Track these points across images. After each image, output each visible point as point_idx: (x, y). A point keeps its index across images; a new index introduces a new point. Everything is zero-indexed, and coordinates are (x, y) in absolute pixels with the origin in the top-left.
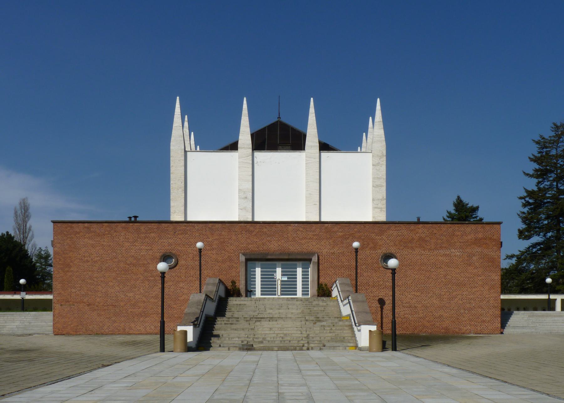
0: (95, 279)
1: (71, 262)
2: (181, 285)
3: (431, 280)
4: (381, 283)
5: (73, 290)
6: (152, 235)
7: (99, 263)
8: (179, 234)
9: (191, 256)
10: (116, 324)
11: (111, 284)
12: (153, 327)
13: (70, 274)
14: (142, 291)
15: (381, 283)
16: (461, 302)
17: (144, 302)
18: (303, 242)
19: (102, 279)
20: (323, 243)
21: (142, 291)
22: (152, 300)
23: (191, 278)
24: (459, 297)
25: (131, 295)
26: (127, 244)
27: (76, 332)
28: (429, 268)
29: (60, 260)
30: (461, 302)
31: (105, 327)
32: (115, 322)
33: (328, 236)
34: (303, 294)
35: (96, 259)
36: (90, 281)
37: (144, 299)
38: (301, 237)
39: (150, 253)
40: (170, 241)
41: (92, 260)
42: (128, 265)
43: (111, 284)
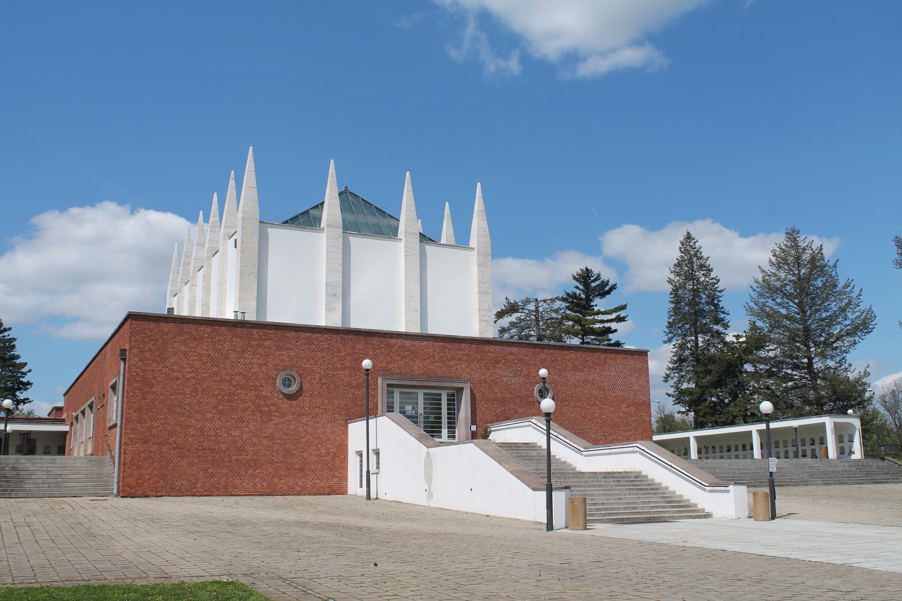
0: (187, 408)
1: (154, 378)
2: (304, 419)
5: (155, 424)
6: (268, 343)
7: (194, 382)
9: (317, 376)
12: (265, 484)
13: (150, 397)
14: (253, 429)
17: (254, 444)
18: (452, 363)
20: (473, 367)
21: (253, 429)
22: (265, 442)
23: (317, 410)
25: (237, 433)
26: (233, 355)
27: (157, 492)
29: (138, 374)
31: (199, 485)
32: (212, 475)
35: (189, 375)
36: (179, 410)
37: (255, 440)
39: (264, 369)
40: (292, 353)
41: (184, 376)
42: (234, 386)
43: (209, 415)
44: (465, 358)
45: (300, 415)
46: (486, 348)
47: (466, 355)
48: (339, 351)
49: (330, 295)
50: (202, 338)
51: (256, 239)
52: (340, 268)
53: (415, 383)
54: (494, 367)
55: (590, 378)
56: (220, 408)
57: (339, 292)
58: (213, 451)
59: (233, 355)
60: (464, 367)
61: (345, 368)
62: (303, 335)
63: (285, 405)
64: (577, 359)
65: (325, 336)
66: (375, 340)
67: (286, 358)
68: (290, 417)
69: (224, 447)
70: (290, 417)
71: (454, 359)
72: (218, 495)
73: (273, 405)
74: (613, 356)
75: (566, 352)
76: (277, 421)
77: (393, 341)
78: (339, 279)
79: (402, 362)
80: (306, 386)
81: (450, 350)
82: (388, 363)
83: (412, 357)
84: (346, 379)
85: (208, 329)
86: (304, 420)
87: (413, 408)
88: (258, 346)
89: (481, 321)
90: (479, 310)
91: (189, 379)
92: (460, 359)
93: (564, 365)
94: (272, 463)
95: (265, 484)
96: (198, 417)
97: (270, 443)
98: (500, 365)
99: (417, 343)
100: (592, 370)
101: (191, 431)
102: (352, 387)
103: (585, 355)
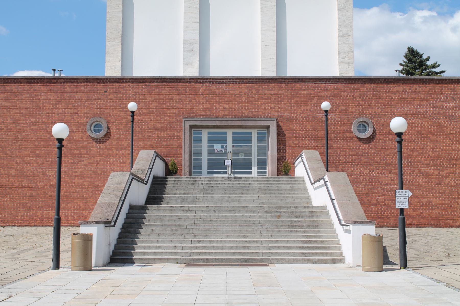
2: (112, 160)
3: (415, 154)
4: (355, 157)
6: (79, 94)
8: (110, 93)
9: (124, 122)
10: (31, 213)
11: (28, 159)
12: (76, 216)
15: (355, 157)
16: (453, 183)
18: (259, 103)
19: (17, 153)
20: (282, 105)
22: (76, 180)
23: (123, 151)
24: (451, 176)
26: (48, 107)
28: (414, 137)
30: (453, 183)
31: (19, 217)
32: (30, 209)
33: (289, 96)
34: (259, 173)
38: (256, 97)
39: (75, 117)
40: (100, 102)
41: (6, 127)
43: (28, 159)
44: (274, 97)
45: (108, 156)
46: (298, 86)
47: (275, 94)
48: (145, 98)
49: (188, 51)
50: (22, 94)
51: (120, 8)
52: (197, 26)
53: (218, 123)
54: (306, 105)
55: (421, 110)
56: (37, 152)
57: (196, 47)
58: (31, 188)
59: (48, 107)
60: (272, 106)
61: (151, 113)
62: (110, 85)
63: (94, 147)
64: (405, 91)
65: (132, 85)
66: (180, 86)
67: (95, 107)
68: (99, 158)
69: (40, 185)
70: (99, 158)
71: (262, 98)
72: (35, 226)
73: (84, 148)
74: (451, 86)
75: (391, 85)
76: (87, 162)
77: (198, 85)
78: (196, 36)
79: (207, 105)
80: (113, 130)
81: (258, 90)
82: (193, 106)
83: (217, 99)
84: (151, 123)
85: (27, 86)
86: (111, 161)
87: (222, 147)
88: (70, 98)
89: (341, 63)
90: (339, 53)
91: (11, 129)
92: (268, 99)
93: (388, 99)
94: (83, 198)
95: (76, 216)
96: (19, 160)
97: (81, 181)
98: (313, 102)
99: (223, 86)
100: (424, 102)
101: (13, 173)
102: (157, 129)
103: (415, 86)
